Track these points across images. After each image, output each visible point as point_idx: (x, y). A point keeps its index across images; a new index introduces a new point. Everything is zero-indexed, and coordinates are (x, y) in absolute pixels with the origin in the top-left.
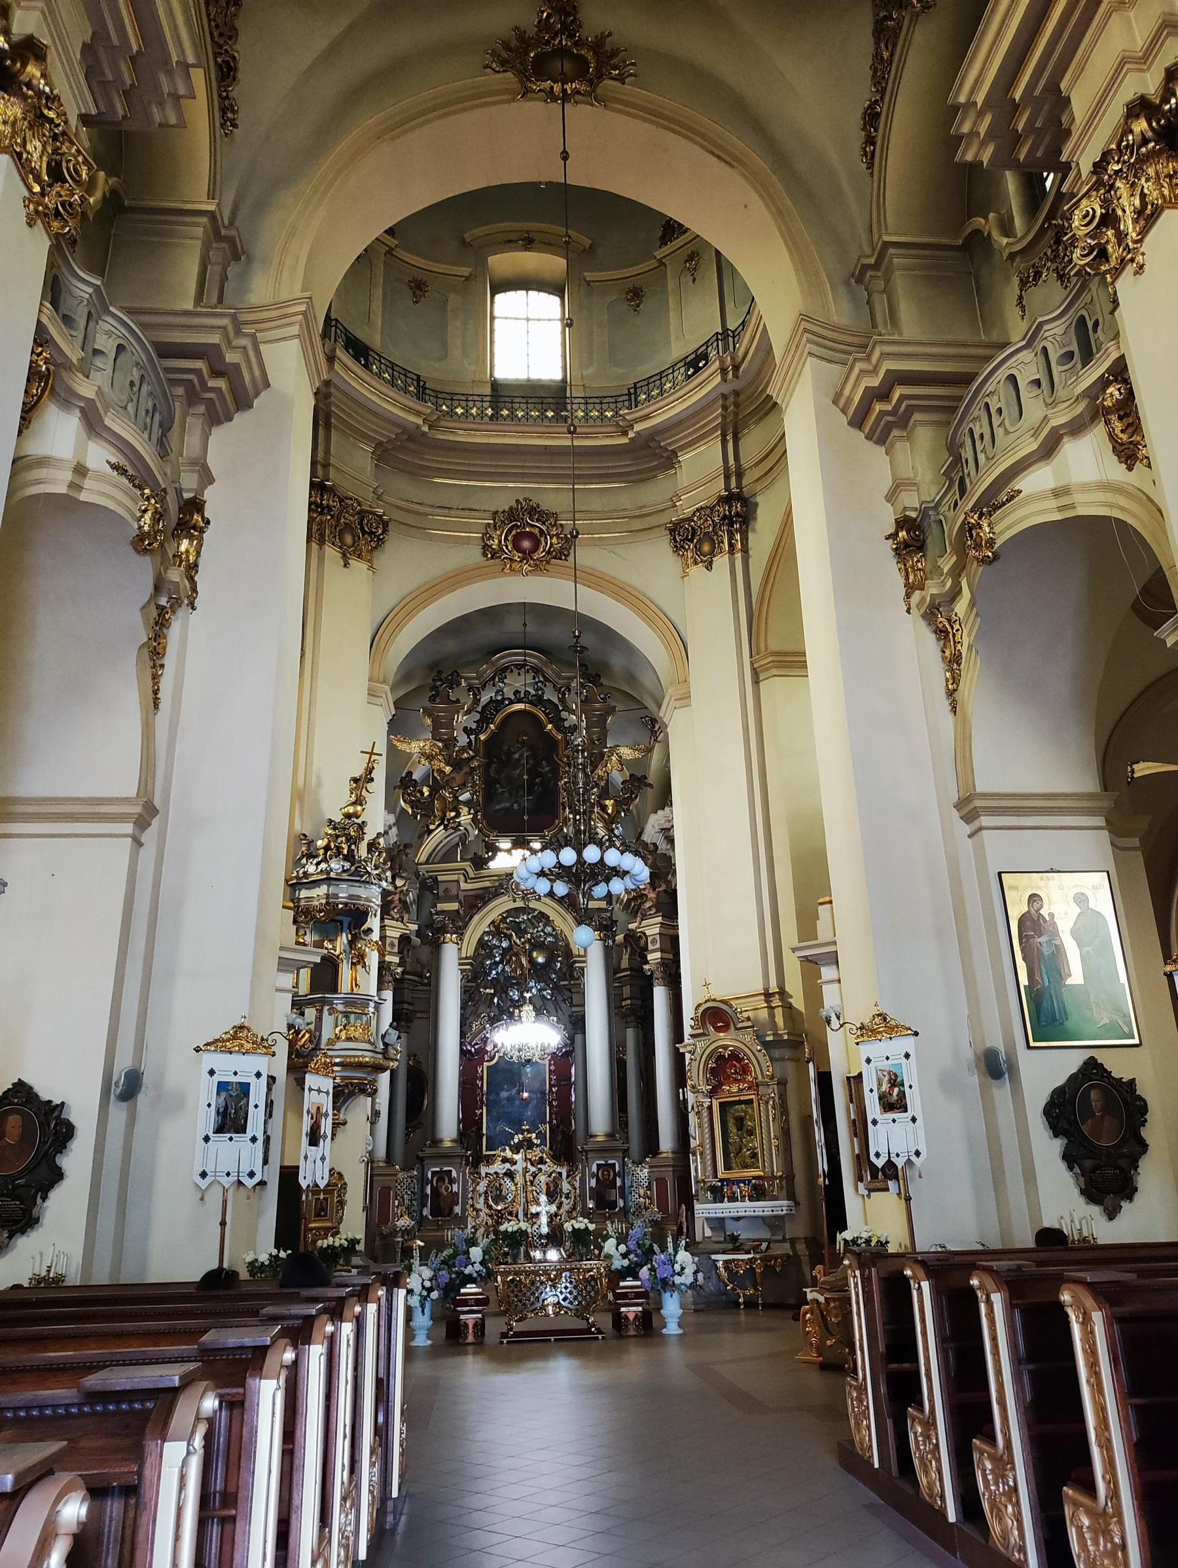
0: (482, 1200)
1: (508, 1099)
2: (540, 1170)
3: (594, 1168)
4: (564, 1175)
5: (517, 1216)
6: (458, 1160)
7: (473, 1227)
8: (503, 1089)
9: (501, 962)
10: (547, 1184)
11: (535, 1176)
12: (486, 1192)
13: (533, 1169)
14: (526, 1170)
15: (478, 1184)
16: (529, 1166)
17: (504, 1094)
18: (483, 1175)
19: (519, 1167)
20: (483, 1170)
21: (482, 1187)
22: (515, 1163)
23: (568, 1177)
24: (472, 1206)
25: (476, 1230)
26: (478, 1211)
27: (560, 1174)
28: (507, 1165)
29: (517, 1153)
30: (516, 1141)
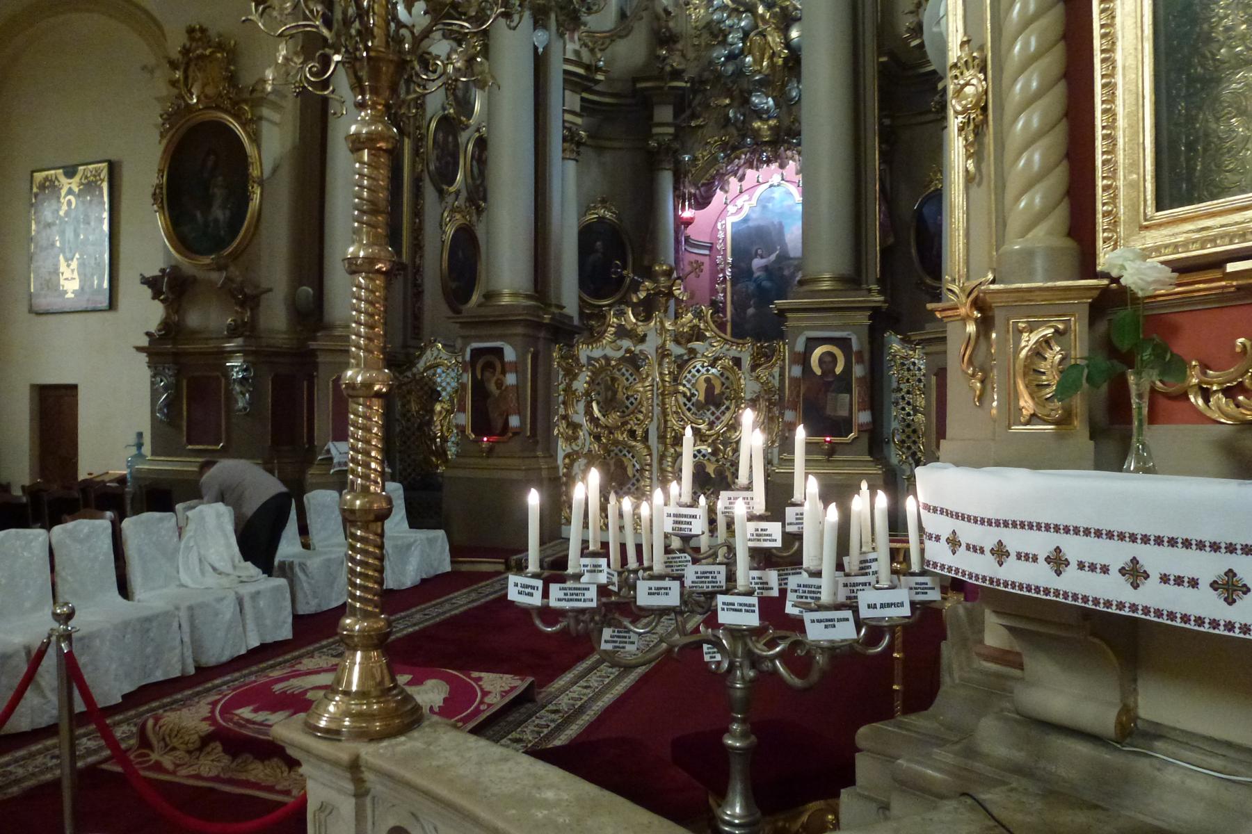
0: (581, 407)
1: (766, 268)
2: (693, 352)
3: (800, 346)
4: (747, 362)
5: (645, 438)
6: (520, 330)
7: (568, 456)
8: (756, 255)
9: (742, 51)
10: (708, 380)
11: (682, 364)
12: (587, 393)
13: (679, 350)
14: (663, 353)
15: (575, 377)
16: (670, 345)
17: (757, 263)
18: (583, 360)
19: (649, 347)
20: (584, 352)
21: (581, 384)
22: (643, 339)
23: (754, 367)
24: (565, 417)
25: (573, 461)
26: (575, 427)
27: (737, 362)
28: (626, 343)
29: (648, 318)
30: (642, 295)
